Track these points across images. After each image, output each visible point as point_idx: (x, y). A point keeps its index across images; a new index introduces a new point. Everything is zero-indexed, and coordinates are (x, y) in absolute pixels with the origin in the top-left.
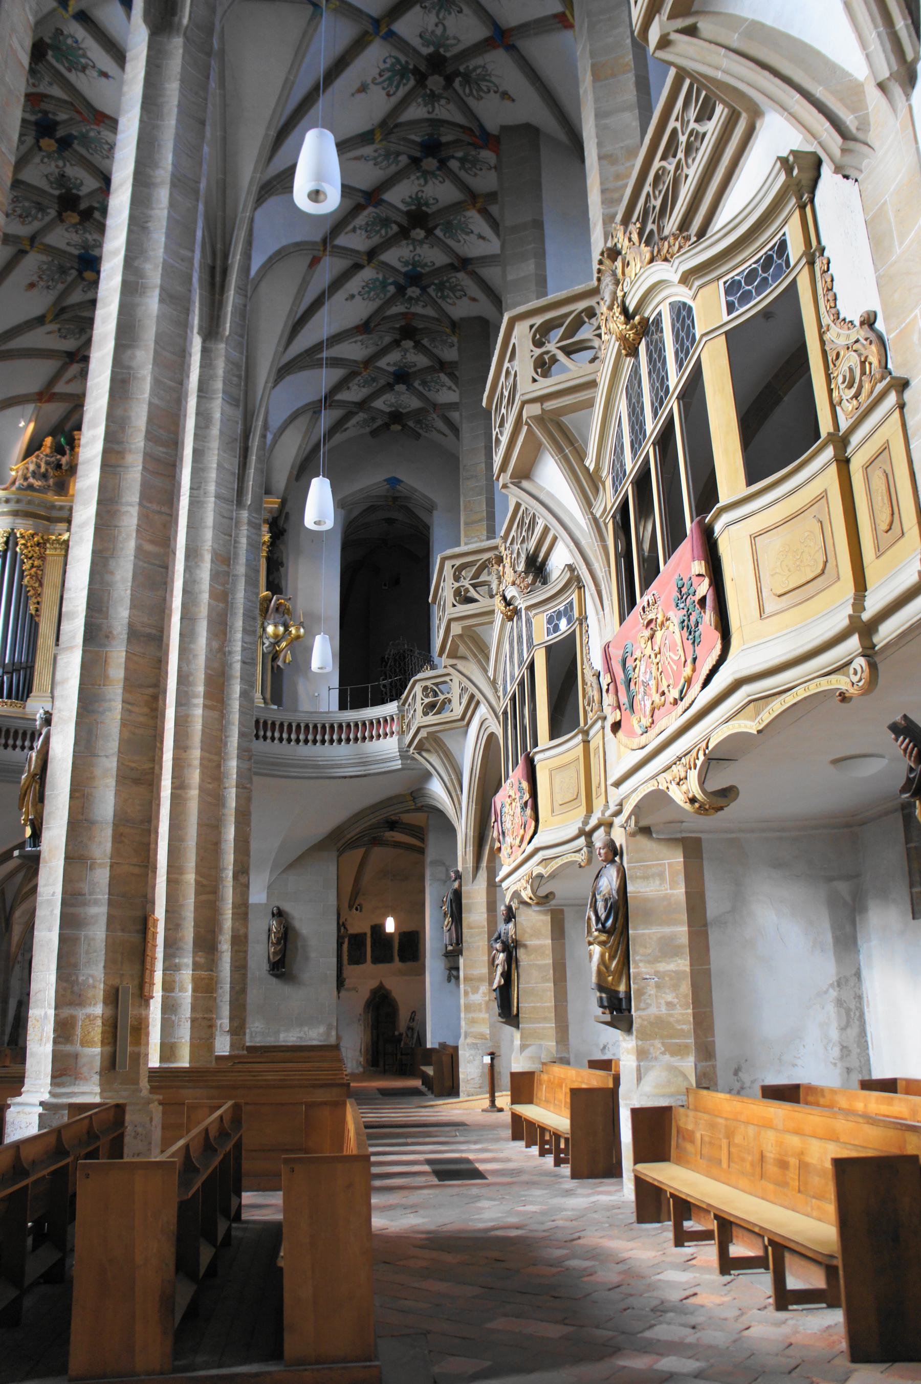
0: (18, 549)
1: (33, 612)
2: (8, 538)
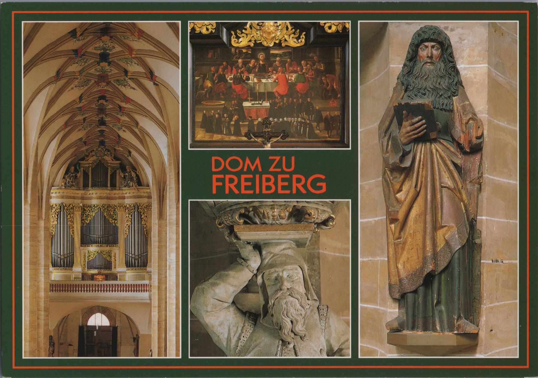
1: (72, 234)
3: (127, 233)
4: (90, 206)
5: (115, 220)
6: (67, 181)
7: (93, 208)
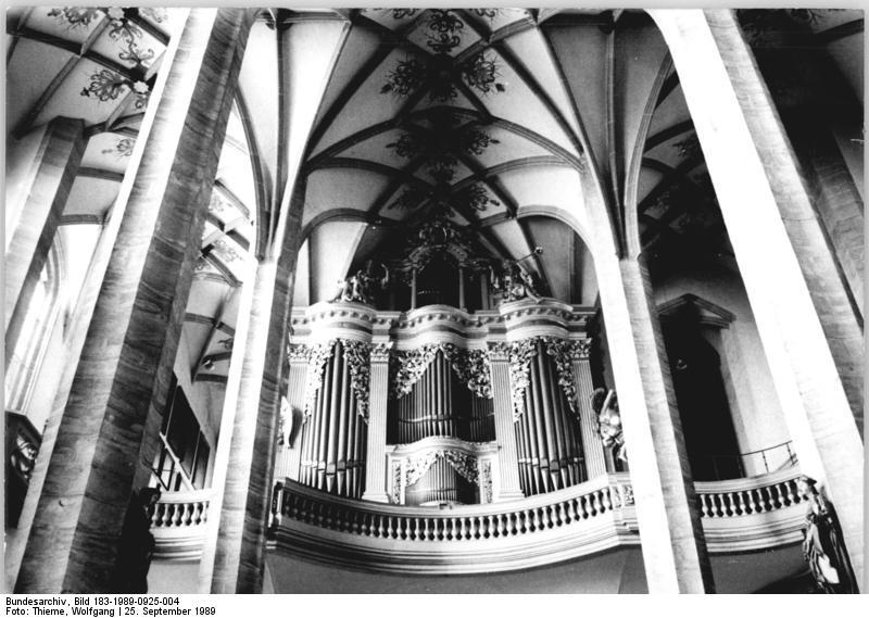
0: (345, 356)
2: (334, 347)
3: (521, 410)
5: (483, 383)
6: (355, 286)
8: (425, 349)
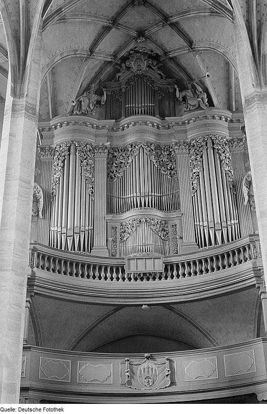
0: (77, 154)
4: (125, 150)
7: (130, 149)
8: (132, 146)
